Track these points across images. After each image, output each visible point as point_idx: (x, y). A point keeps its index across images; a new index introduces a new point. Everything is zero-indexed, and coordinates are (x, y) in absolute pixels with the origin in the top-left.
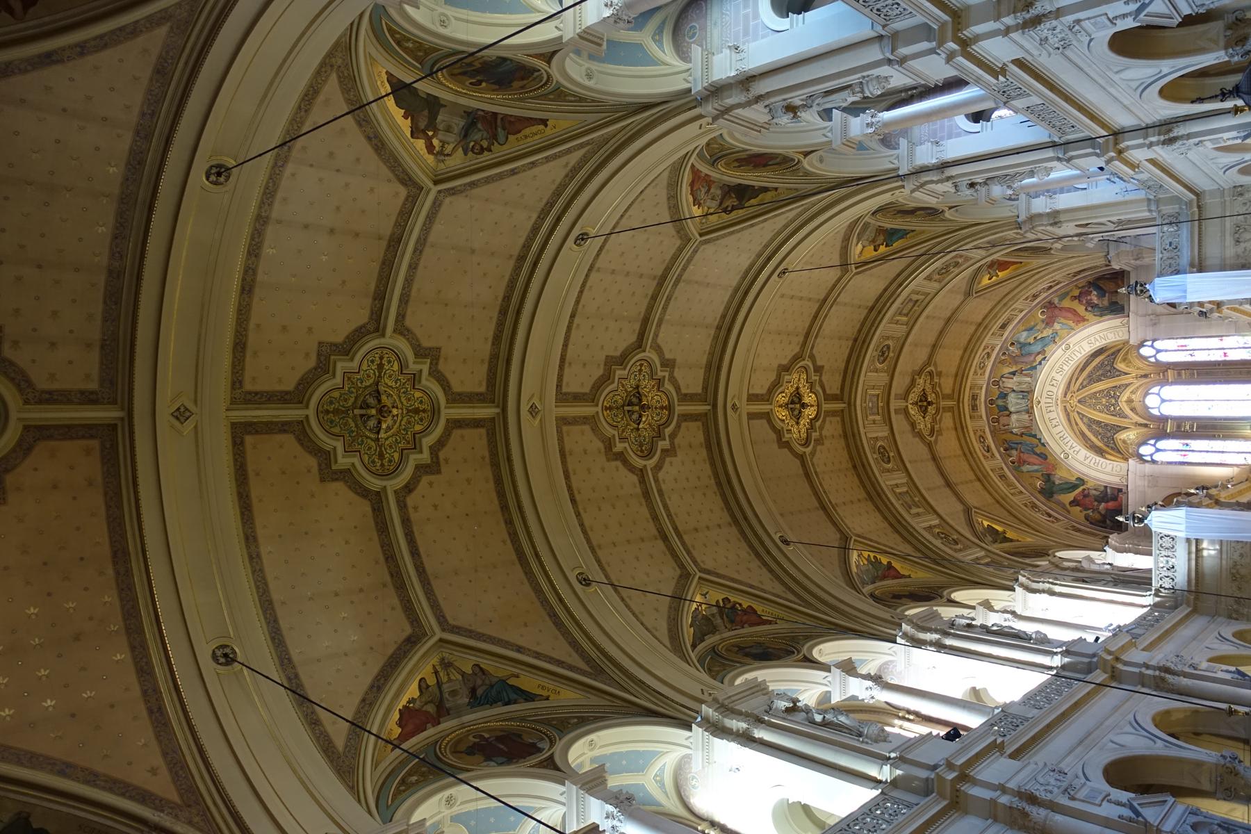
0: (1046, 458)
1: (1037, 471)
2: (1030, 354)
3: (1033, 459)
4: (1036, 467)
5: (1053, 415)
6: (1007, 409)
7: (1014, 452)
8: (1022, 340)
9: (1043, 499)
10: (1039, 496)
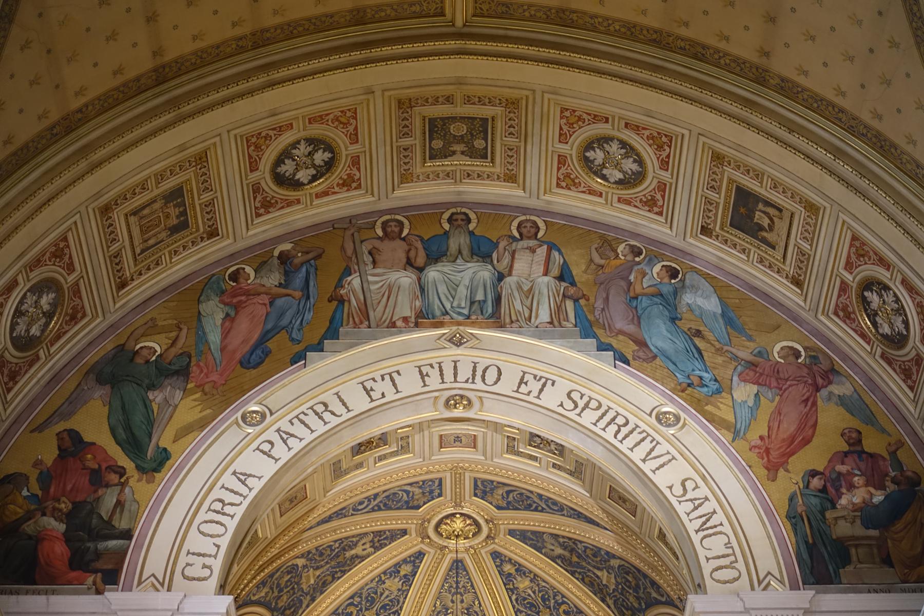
0: (246, 364)
1: (201, 337)
2: (637, 320)
3: (247, 330)
4: (214, 337)
5: (409, 384)
6: (434, 258)
7: (273, 279)
8: (688, 298)
9: (92, 357)
10: (108, 345)
